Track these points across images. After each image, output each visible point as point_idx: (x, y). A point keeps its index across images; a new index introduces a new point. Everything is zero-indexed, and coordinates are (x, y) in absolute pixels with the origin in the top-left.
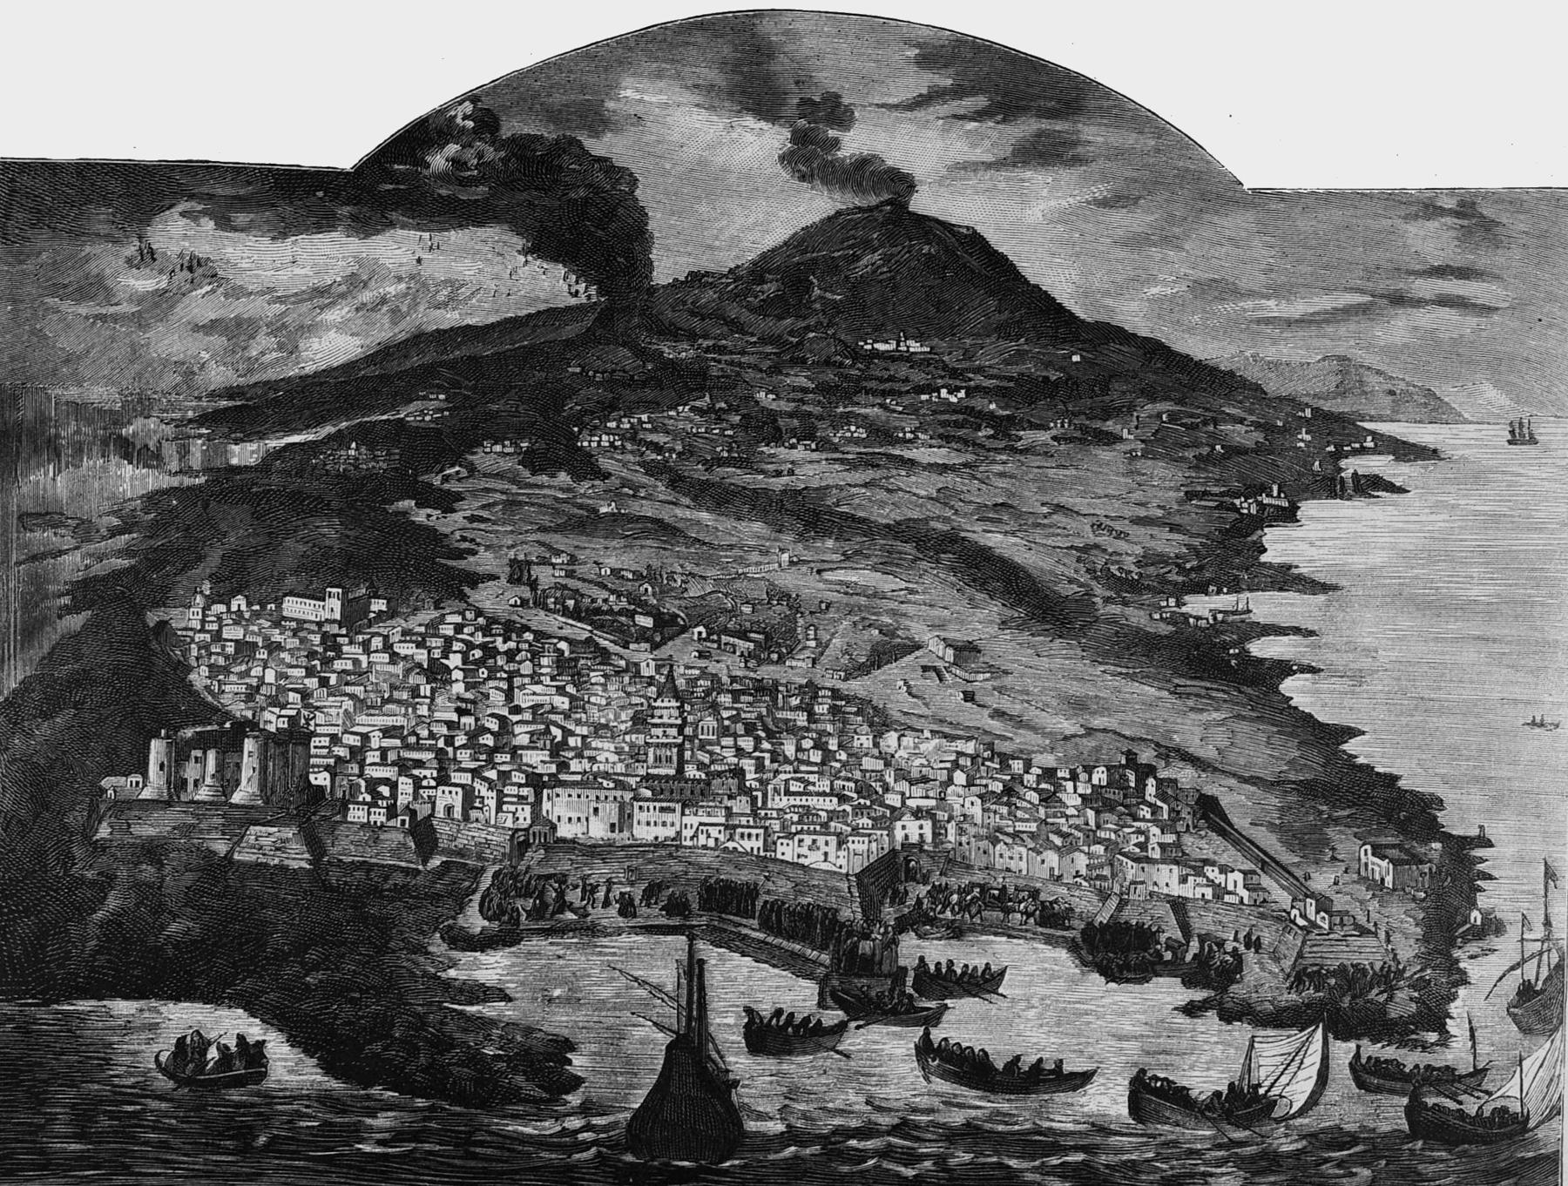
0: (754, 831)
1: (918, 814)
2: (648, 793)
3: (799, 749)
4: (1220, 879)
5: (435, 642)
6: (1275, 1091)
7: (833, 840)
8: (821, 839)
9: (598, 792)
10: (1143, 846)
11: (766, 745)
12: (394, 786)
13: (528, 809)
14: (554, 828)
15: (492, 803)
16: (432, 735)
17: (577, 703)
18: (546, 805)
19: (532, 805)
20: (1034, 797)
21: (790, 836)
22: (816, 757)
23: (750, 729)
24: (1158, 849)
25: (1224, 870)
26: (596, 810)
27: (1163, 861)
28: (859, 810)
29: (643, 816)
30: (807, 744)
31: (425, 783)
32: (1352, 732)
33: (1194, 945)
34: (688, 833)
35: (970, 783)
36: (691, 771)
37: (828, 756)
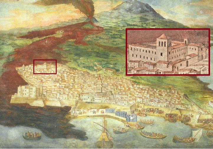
0: (114, 101)
1: (140, 98)
2: (97, 95)
3: (121, 88)
4: (187, 106)
5: (62, 72)
6: (195, 138)
7: (126, 102)
8: (124, 102)
9: (88, 95)
10: (175, 102)
11: (115, 87)
12: (56, 94)
13: (78, 98)
14: (82, 100)
15: (72, 97)
16: (62, 86)
17: (85, 82)
18: (81, 97)
19: (79, 97)
20: (158, 95)
21: (119, 101)
22: (123, 89)
23: (112, 85)
24: (177, 102)
25: (188, 105)
26: (89, 97)
27: (178, 104)
28: (130, 97)
29: (96, 98)
30: (122, 87)
31: (61, 94)
32: (208, 84)
33: (183, 117)
34: (103, 101)
35: (148, 93)
36: (103, 91)
37: (125, 88)
